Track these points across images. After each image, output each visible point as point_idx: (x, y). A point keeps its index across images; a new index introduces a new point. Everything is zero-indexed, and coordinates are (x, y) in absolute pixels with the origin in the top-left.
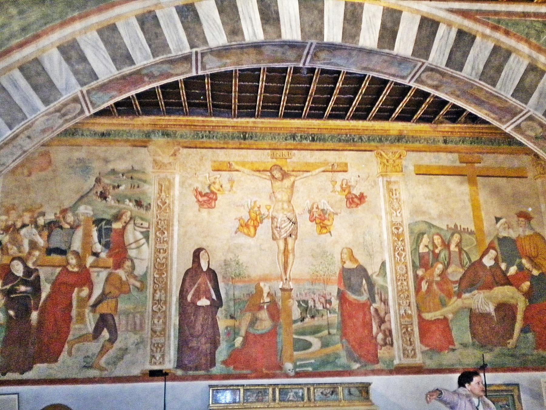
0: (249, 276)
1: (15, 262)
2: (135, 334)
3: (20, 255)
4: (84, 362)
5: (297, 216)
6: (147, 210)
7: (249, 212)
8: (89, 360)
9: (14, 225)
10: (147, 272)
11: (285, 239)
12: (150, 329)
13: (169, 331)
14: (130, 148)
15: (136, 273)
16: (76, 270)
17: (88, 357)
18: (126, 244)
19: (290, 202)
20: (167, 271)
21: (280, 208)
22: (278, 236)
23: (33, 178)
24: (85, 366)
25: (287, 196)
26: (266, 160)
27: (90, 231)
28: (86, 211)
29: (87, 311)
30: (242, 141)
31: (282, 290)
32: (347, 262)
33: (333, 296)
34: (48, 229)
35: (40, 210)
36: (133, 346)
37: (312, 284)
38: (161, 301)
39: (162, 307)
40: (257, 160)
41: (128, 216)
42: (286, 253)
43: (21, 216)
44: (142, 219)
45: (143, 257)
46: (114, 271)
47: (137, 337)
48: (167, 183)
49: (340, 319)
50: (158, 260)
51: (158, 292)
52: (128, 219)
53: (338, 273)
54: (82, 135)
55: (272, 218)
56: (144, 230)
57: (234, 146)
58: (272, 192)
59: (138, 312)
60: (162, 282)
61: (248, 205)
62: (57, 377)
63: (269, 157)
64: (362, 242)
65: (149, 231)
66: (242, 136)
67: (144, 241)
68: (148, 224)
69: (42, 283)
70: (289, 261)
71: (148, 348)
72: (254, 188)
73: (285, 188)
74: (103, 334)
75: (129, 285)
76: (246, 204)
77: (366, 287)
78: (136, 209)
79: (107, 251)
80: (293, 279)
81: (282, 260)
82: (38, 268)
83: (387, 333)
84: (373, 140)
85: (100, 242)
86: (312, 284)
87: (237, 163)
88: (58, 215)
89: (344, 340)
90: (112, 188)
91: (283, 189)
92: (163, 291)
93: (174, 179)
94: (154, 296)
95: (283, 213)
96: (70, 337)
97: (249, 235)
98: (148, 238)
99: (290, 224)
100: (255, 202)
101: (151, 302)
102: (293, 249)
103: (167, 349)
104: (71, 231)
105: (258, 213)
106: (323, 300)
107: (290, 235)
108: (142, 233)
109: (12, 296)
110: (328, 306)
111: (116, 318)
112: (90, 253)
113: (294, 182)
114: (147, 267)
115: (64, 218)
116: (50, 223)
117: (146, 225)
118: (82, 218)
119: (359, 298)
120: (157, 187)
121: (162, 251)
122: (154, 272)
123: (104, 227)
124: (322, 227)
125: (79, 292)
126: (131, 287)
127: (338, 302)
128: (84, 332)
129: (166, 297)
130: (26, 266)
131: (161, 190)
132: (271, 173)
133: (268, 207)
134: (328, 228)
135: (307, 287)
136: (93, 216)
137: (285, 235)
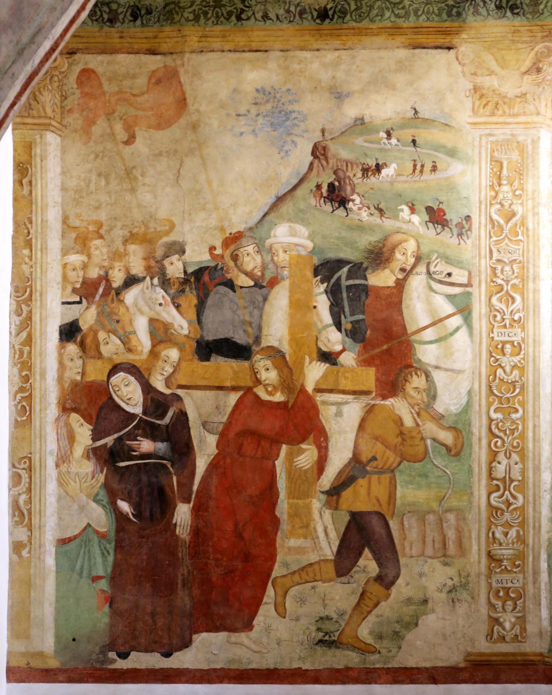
2: (446, 564)
3: (130, 358)
4: (319, 629)
6: (460, 235)
8: (328, 626)
10: (468, 405)
13: (537, 559)
15: (440, 407)
16: (279, 397)
17: (329, 618)
20: (523, 404)
24: (321, 641)
28: (295, 240)
34: (197, 289)
36: (443, 596)
38: (512, 481)
39: (514, 497)
41: (409, 253)
44: (448, 260)
45: (457, 366)
46: (378, 402)
47: (451, 571)
48: (515, 156)
50: (500, 371)
51: (501, 457)
52: (412, 260)
56: (456, 290)
59: (449, 510)
60: (513, 431)
62: (253, 666)
65: (469, 294)
68: (466, 273)
69: (196, 431)
74: (361, 562)
75: (422, 439)
78: (431, 232)
79: (358, 347)
82: (180, 392)
88: (218, 251)
90: (360, 174)
92: (515, 457)
93: (535, 142)
94: (490, 470)
96: (277, 571)
98: (470, 313)
101: (484, 482)
103: (530, 605)
104: (258, 295)
111: (393, 524)
112: (315, 355)
114: (469, 393)
115: (235, 258)
116: (199, 273)
117: (460, 276)
118: (282, 258)
120: (486, 168)
123: (345, 283)
126: (429, 442)
128: (313, 558)
129: (523, 472)
131: (500, 178)
136: (313, 252)
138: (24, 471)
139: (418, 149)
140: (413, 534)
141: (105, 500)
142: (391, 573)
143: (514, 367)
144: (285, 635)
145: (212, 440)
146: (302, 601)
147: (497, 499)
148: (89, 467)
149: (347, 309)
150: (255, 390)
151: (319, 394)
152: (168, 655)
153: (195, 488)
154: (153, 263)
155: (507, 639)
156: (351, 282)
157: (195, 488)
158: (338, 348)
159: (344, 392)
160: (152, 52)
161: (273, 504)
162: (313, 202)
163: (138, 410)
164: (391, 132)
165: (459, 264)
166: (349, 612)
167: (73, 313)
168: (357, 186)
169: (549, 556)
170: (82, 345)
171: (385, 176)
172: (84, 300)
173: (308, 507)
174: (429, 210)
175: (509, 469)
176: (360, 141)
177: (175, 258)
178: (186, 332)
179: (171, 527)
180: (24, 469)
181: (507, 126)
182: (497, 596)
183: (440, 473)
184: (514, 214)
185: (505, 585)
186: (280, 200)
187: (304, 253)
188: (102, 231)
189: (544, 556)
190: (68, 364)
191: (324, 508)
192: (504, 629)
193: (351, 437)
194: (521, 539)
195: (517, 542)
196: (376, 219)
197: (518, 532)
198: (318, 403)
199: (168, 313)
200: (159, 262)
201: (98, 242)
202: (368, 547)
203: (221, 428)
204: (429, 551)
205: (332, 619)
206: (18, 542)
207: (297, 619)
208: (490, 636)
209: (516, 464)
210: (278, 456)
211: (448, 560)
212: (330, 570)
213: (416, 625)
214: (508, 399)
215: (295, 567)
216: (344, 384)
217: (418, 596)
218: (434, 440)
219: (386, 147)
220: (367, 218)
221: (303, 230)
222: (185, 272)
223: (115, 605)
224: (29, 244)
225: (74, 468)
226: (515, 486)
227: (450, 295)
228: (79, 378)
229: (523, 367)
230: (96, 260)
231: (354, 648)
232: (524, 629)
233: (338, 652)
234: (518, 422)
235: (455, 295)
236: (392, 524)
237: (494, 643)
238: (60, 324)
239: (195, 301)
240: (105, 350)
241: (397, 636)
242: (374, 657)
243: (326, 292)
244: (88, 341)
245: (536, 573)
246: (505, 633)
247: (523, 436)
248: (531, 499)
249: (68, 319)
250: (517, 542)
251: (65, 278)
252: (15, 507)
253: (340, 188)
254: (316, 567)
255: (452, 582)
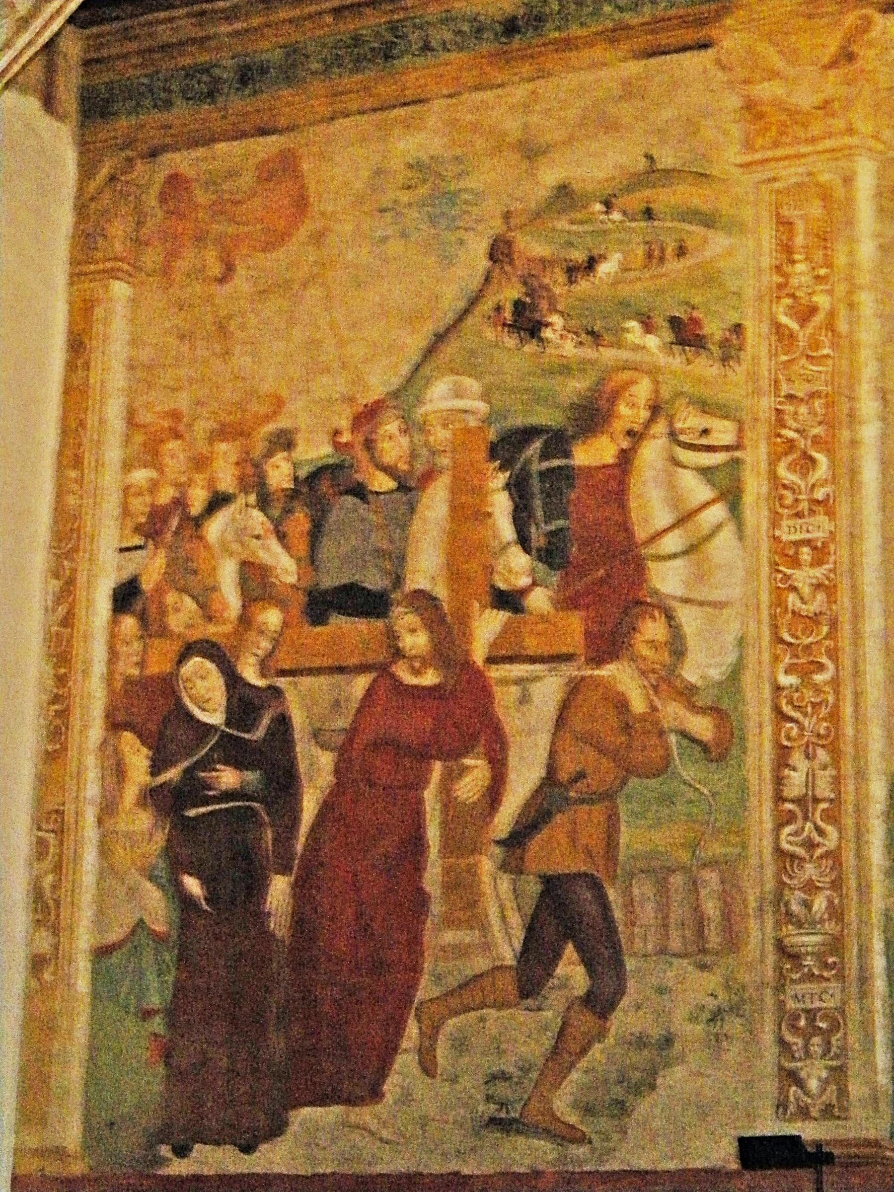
1: (195, 662)
2: (703, 967)
3: (212, 631)
4: (489, 1098)
6: (725, 360)
8: (502, 1090)
9: (180, 503)
12: (770, 948)
13: (864, 951)
14: (634, 68)
15: (690, 674)
16: (430, 678)
17: (504, 1076)
18: (641, 534)
20: (833, 654)
23: (241, 282)
24: (493, 1121)
27: (480, 492)
29: (487, 865)
35: (270, 427)
41: (642, 402)
43: (200, 463)
44: (705, 407)
47: (712, 981)
50: (792, 599)
51: (797, 758)
52: (644, 414)
54: (427, 47)
56: (719, 458)
67: (717, 512)
71: (768, 1037)
74: (561, 970)
75: (661, 733)
78: (676, 361)
79: (555, 578)
82: (282, 682)
85: (523, 541)
88: (345, 438)
96: (426, 990)
103: (854, 1040)
108: (705, 472)
109: (192, 813)
114: (741, 642)
115: (369, 445)
120: (767, 236)
121: (805, 553)
122: (776, 659)
125: (450, 778)
126: (673, 739)
128: (481, 964)
130: (233, 680)
136: (487, 421)
138: (52, 835)
139: (656, 223)
140: (648, 913)
141: (163, 874)
142: (608, 986)
143: (818, 586)
144: (431, 1109)
145: (326, 760)
146: (460, 1045)
147: (791, 838)
148: (144, 820)
149: (539, 513)
150: (393, 669)
151: (494, 667)
152: (247, 1149)
153: (299, 848)
154: (250, 470)
155: (814, 1113)
156: (546, 465)
157: (299, 848)
158: (524, 581)
159: (533, 660)
160: (263, 132)
161: (419, 869)
162: (490, 334)
163: (215, 718)
164: (613, 200)
165: (723, 411)
166: (540, 1062)
167: (132, 564)
168: (559, 299)
169: (888, 944)
170: (143, 619)
171: (604, 276)
172: (151, 542)
173: (472, 871)
174: (675, 323)
175: (811, 779)
176: (562, 224)
177: (280, 458)
178: (292, 579)
179: (261, 917)
180: (52, 831)
181: (803, 161)
182: (794, 1028)
183: (691, 795)
184: (813, 310)
185: (809, 1006)
186: (440, 338)
187: (473, 423)
188: (181, 428)
189: (878, 945)
190: (123, 649)
191: (500, 873)
192: (807, 1093)
193: (543, 740)
194: (836, 913)
195: (830, 919)
196: (589, 353)
197: (830, 902)
198: (492, 682)
199: (267, 549)
200: (257, 466)
201: (173, 445)
202: (574, 942)
203: (340, 739)
204: (675, 944)
205: (510, 1078)
206: (36, 956)
207: (454, 1080)
208: (781, 1105)
209: (825, 768)
210: (427, 782)
211: (708, 959)
212: (507, 984)
213: (653, 1087)
214: (808, 647)
215: (452, 982)
216: (532, 645)
217: (655, 1033)
218: (684, 734)
219: (605, 227)
220: (575, 351)
221: (472, 384)
222: (296, 479)
223: (174, 1061)
224: (77, 462)
225: (122, 825)
226: (823, 810)
227: (709, 468)
228: (135, 672)
229: (835, 586)
230: (170, 475)
231: (548, 1134)
232: (843, 1092)
233: (521, 1141)
234: (827, 689)
235: (717, 467)
236: (612, 894)
237: (789, 1121)
238: (113, 586)
239: (307, 526)
240: (176, 623)
241: (621, 1109)
242: (581, 1151)
243: (507, 486)
244: (153, 610)
245: (864, 979)
246: (809, 1101)
247: (834, 716)
248: (851, 833)
249: (125, 575)
250: (830, 919)
251: (126, 512)
252: (37, 895)
253: (534, 307)
254: (487, 982)
255: (716, 1002)
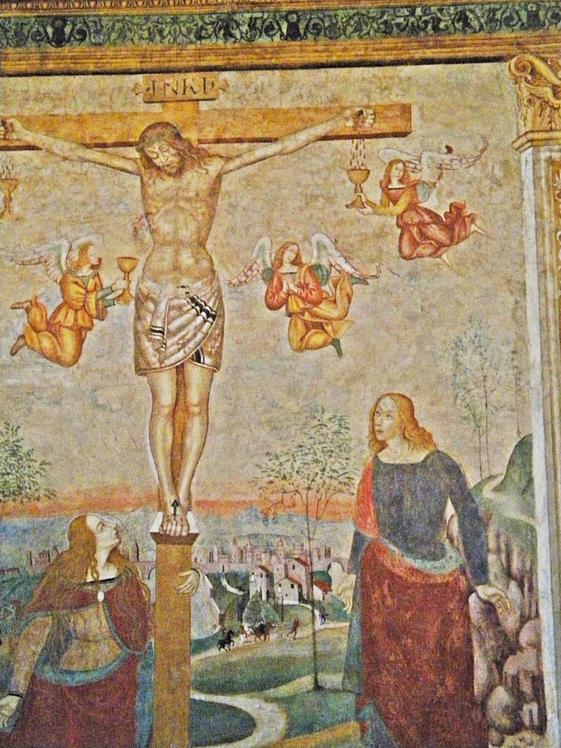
0: (50, 495)
5: (225, 290)
7: (63, 284)
11: (180, 369)
19: (202, 244)
21: (167, 265)
22: (154, 360)
25: (192, 226)
26: (129, 109)
30: (51, 49)
31: (159, 537)
32: (391, 443)
33: (338, 560)
37: (266, 519)
40: (99, 111)
42: (180, 414)
49: (357, 639)
53: (357, 481)
55: (137, 299)
57: (23, 67)
58: (142, 212)
61: (59, 257)
63: (140, 99)
64: (450, 373)
66: (50, 30)
70: (188, 441)
72: (84, 204)
73: (188, 200)
76: (54, 254)
77: (455, 528)
80: (199, 503)
81: (164, 440)
83: (526, 687)
84: (508, 21)
86: (266, 519)
87: (28, 122)
89: (368, 711)
91: (182, 204)
95: (176, 281)
97: (58, 360)
99: (200, 319)
100: (84, 249)
102: (205, 401)
105: (91, 284)
106: (300, 573)
107: (197, 358)
110: (318, 593)
113: (219, 178)
119: (427, 566)
124: (308, 326)
127: (353, 577)
132: (141, 150)
133: (127, 265)
134: (329, 329)
135: (248, 529)
137: (181, 354)
